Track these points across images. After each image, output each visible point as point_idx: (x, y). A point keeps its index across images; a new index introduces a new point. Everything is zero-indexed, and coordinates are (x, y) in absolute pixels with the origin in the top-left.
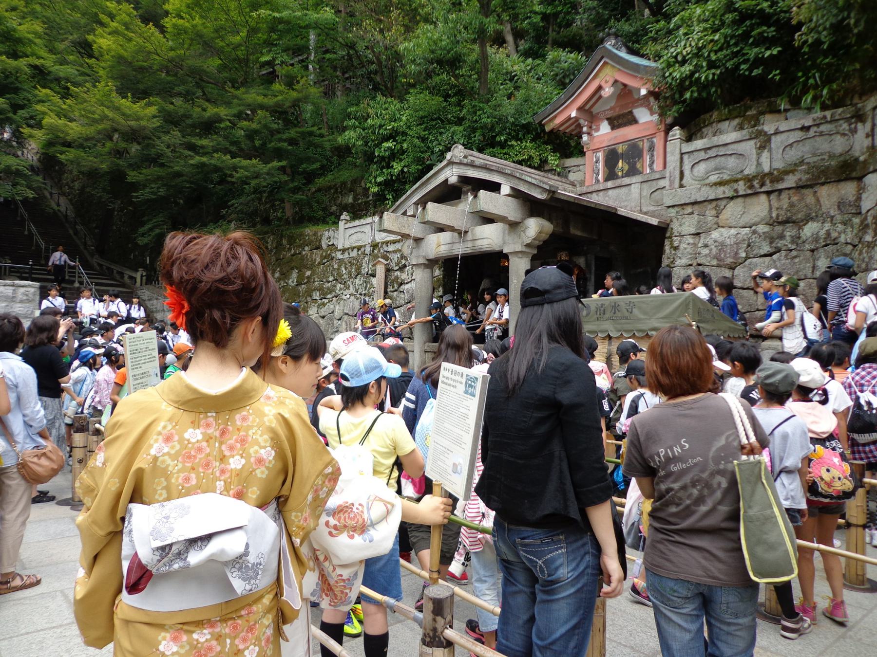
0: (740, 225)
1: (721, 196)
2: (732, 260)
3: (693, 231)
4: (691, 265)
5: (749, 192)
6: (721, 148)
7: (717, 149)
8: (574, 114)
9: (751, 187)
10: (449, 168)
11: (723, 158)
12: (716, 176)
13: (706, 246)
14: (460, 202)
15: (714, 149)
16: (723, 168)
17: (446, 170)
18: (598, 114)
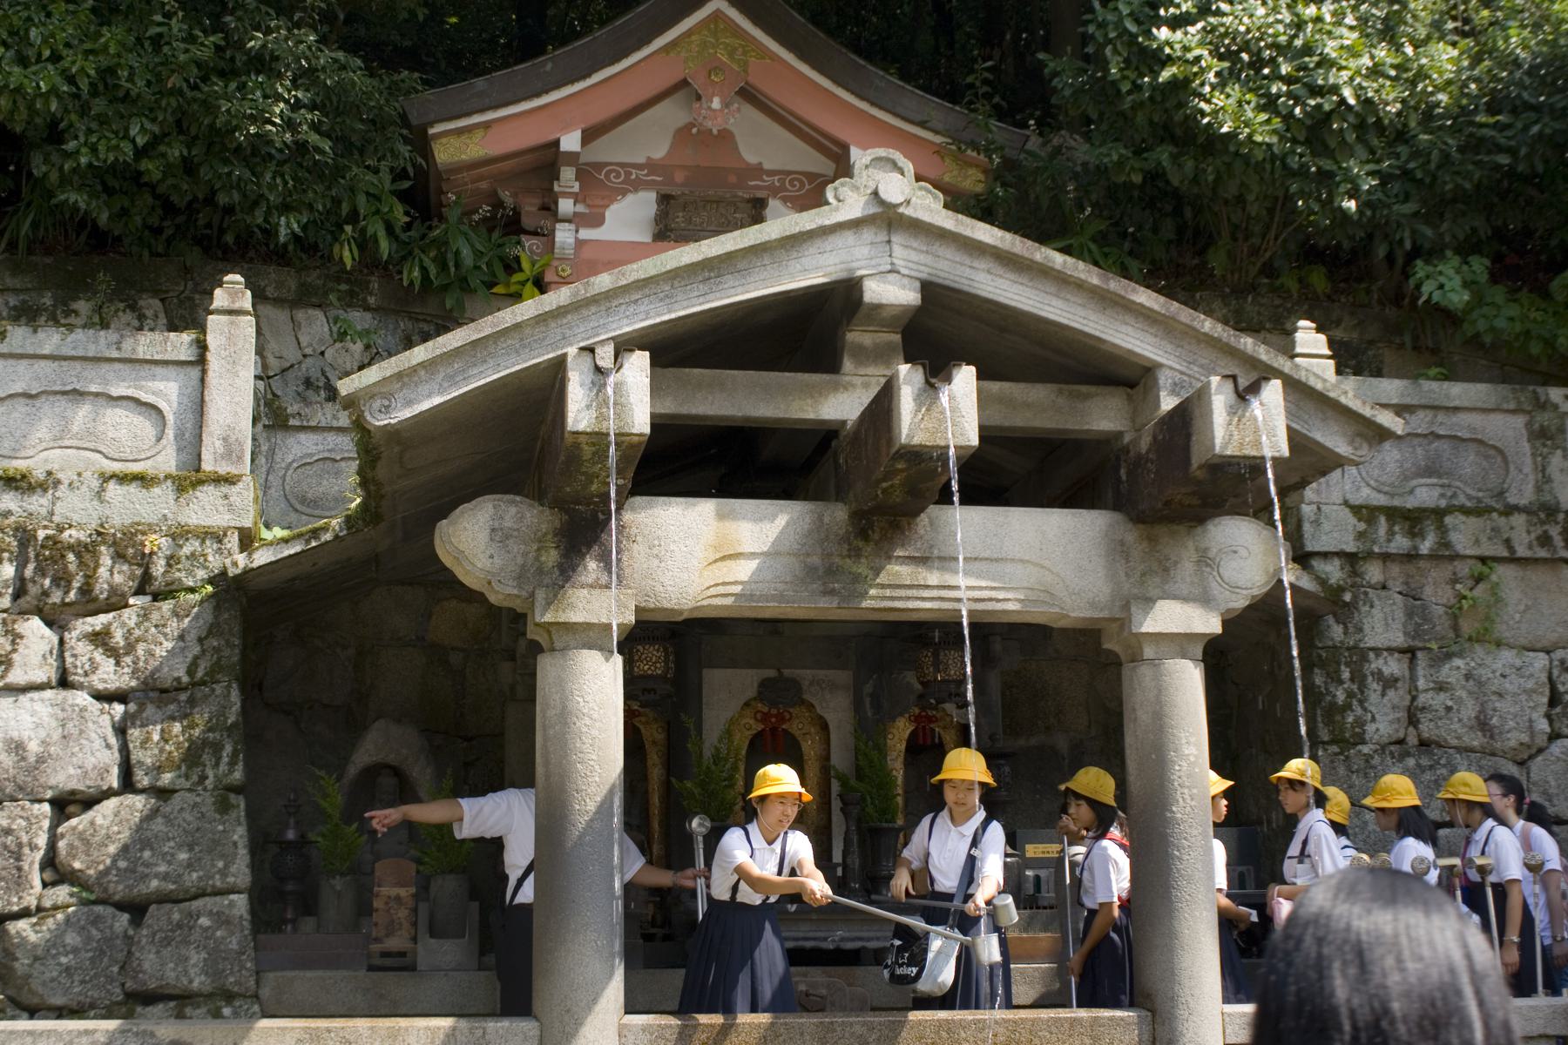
0: (1523, 641)
1: (1468, 552)
2: (1525, 738)
3: (1399, 639)
4: (1401, 742)
5: (1542, 553)
6: (1441, 417)
7: (1430, 414)
8: (570, 142)
9: (1545, 540)
10: (868, 234)
11: (1444, 446)
12: (1436, 492)
13: (1441, 687)
14: (836, 387)
15: (1421, 414)
16: (1449, 474)
17: (849, 238)
18: (599, 166)
